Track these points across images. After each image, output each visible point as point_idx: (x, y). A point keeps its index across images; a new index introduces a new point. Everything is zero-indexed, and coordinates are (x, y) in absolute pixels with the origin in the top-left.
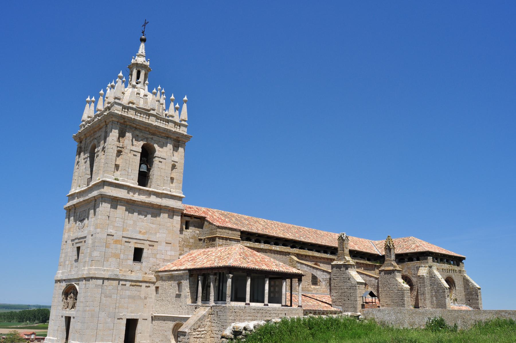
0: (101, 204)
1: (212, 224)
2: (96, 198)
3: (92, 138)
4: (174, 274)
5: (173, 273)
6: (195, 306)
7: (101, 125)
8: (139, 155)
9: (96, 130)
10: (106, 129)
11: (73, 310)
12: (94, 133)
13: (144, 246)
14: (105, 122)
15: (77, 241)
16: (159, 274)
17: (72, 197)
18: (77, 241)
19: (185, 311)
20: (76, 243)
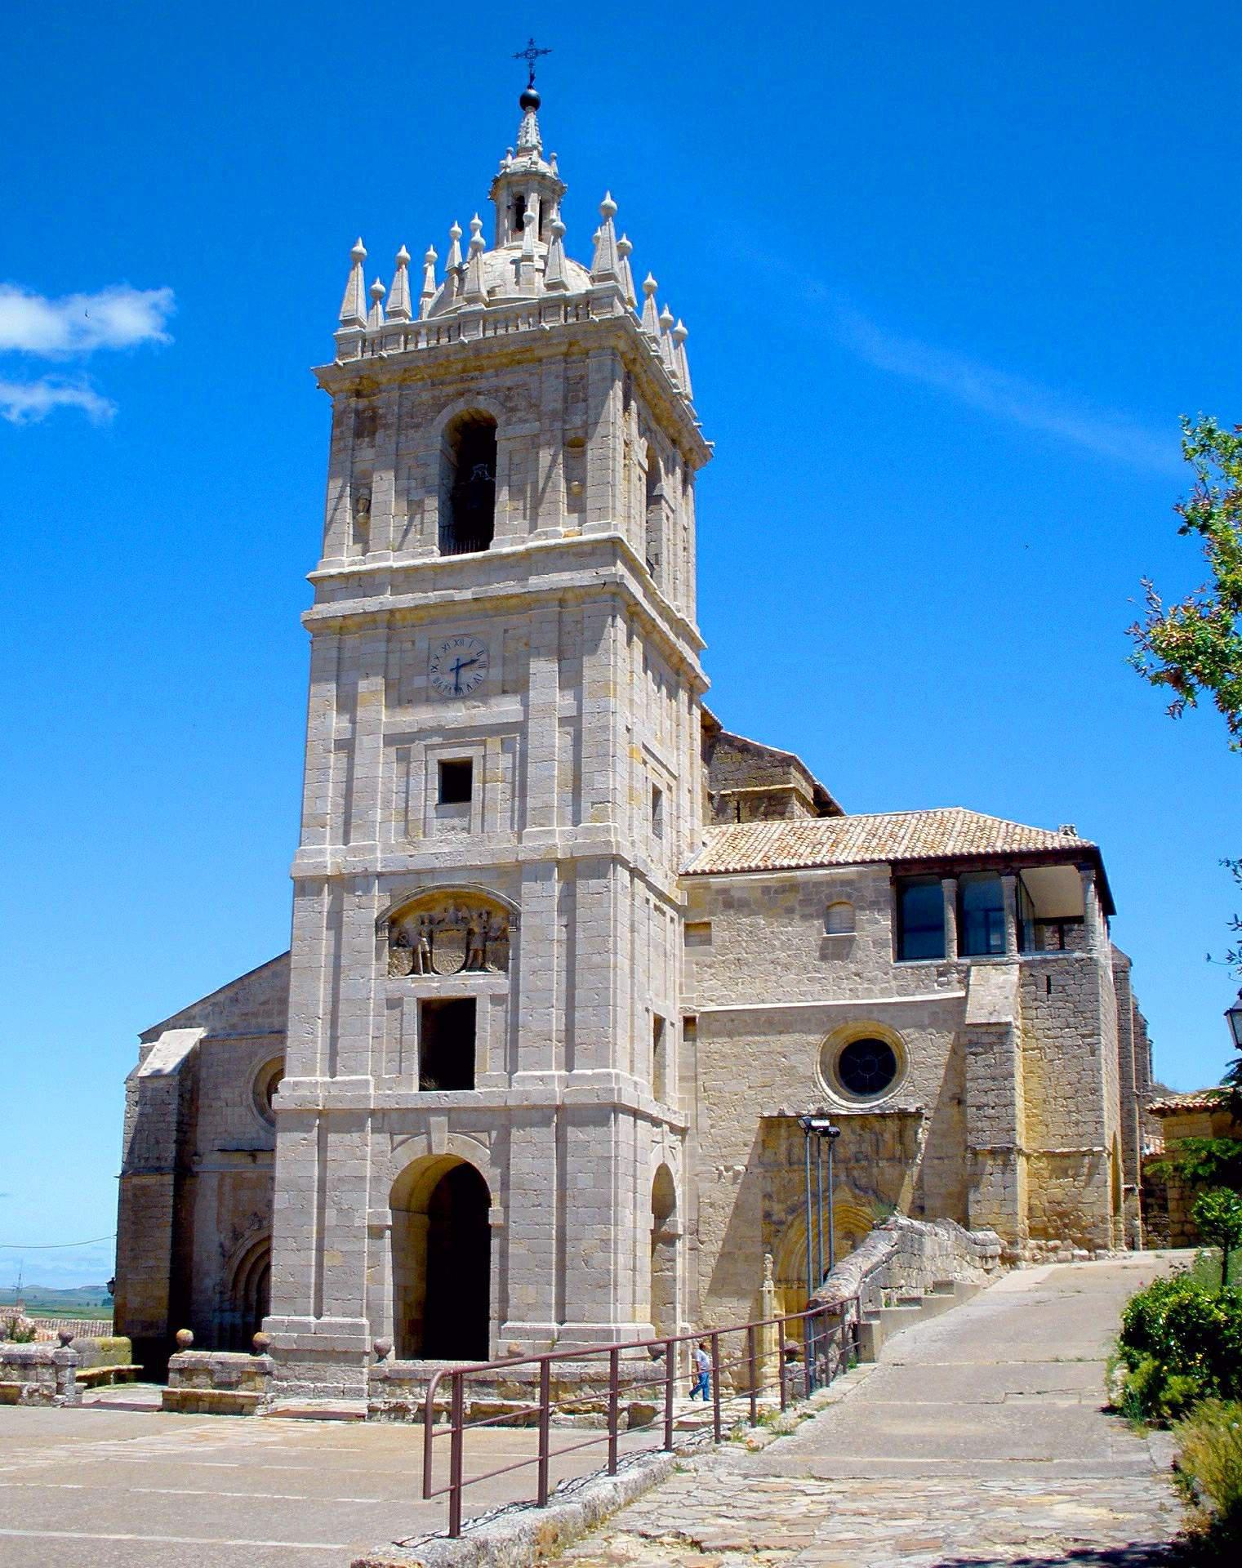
0: (610, 619)
1: (759, 753)
2: (569, 595)
3: (450, 389)
4: (800, 879)
5: (798, 873)
6: (938, 966)
7: (539, 353)
8: (644, 477)
9: (485, 362)
10: (566, 369)
11: (463, 973)
12: (464, 371)
13: (662, 787)
14: (571, 345)
15: (437, 740)
16: (711, 880)
17: (326, 588)
18: (437, 740)
19: (887, 985)
20: (428, 748)
